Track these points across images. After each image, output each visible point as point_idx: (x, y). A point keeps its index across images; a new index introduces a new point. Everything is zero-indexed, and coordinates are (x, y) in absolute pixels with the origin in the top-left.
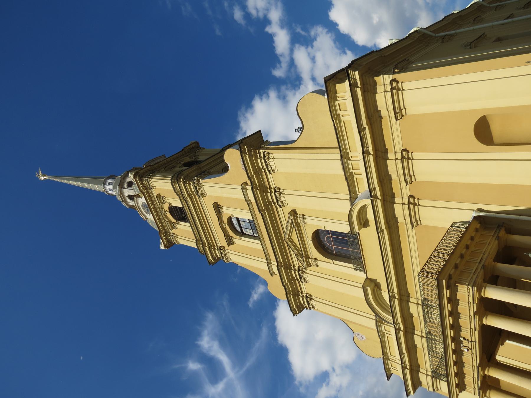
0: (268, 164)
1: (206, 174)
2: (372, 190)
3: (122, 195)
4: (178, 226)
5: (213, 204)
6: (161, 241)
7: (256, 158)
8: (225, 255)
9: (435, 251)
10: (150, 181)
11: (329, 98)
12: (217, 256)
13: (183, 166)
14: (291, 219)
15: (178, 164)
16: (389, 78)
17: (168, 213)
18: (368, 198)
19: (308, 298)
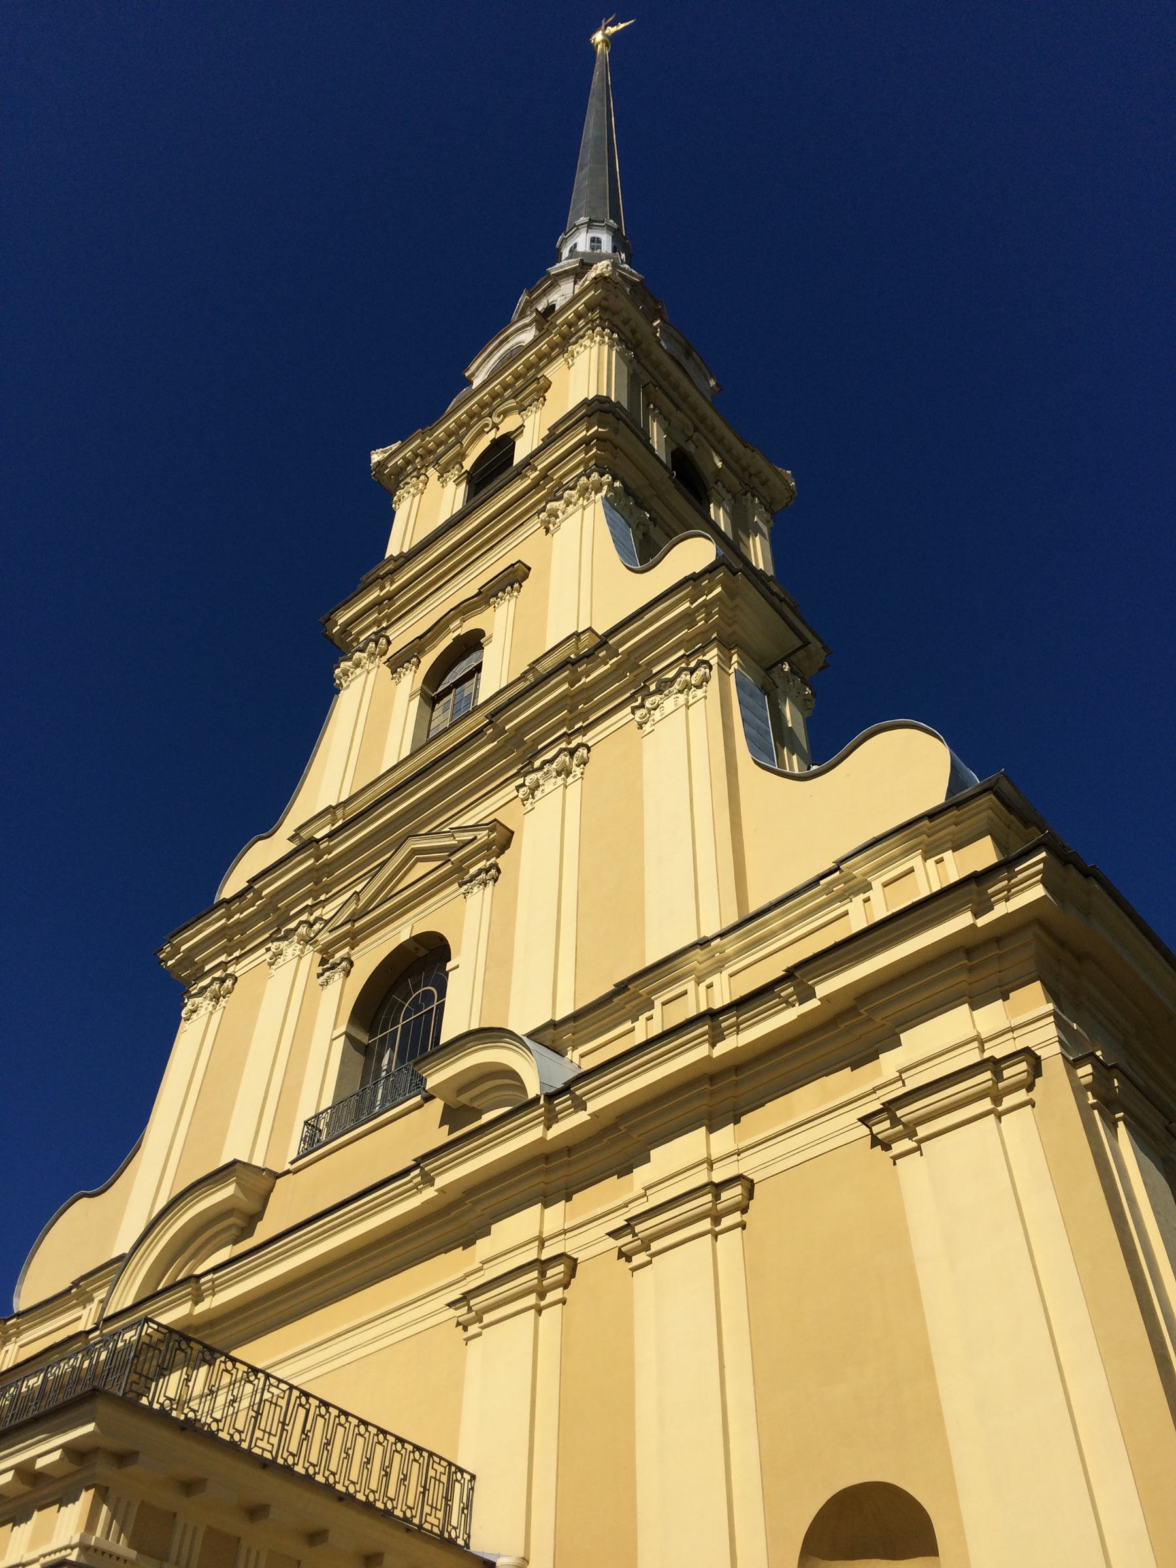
0: (666, 692)
3: (551, 285)
4: (451, 485)
5: (519, 561)
6: (394, 446)
9: (296, 1393)
10: (592, 339)
11: (926, 822)
13: (675, 447)
14: (475, 838)
15: (684, 434)
16: (1045, 1044)
17: (493, 435)
18: (542, 1084)
19: (220, 987)
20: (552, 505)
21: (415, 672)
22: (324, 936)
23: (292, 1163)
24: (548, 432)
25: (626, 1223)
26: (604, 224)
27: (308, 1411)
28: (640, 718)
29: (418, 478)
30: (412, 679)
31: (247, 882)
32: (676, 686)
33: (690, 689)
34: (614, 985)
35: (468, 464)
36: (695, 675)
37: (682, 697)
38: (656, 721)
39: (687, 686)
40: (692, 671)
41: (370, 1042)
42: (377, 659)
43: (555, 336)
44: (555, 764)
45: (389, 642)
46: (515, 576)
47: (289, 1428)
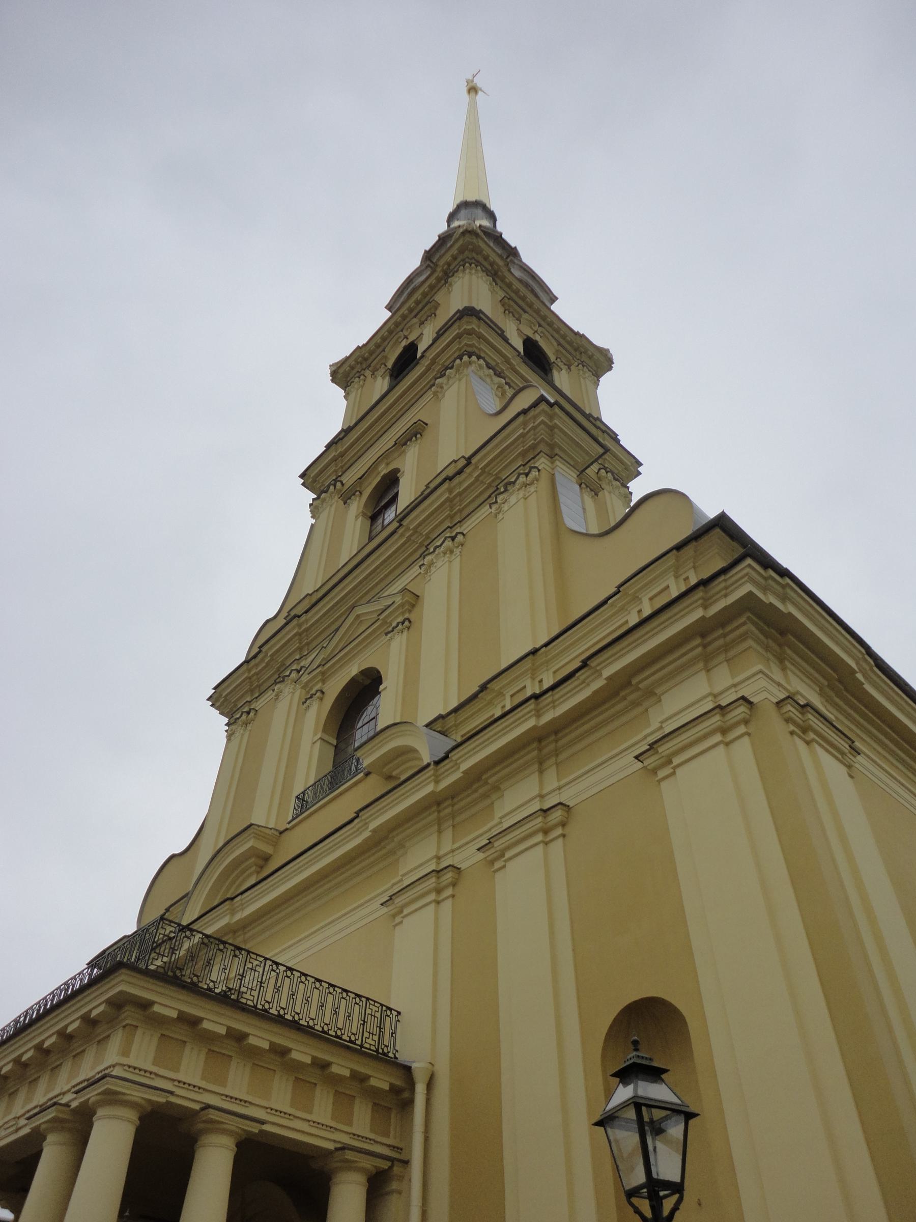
1: (492, 380)
4: (379, 379)
5: (419, 420)
8: (324, 500)
13: (525, 337)
15: (532, 329)
17: (404, 343)
18: (431, 754)
23: (289, 823)
25: (488, 841)
27: (278, 974)
30: (356, 506)
32: (517, 486)
33: (526, 487)
34: (479, 686)
35: (390, 364)
36: (528, 477)
37: (521, 493)
39: (526, 485)
40: (527, 475)
44: (442, 547)
45: (343, 484)
47: (265, 985)
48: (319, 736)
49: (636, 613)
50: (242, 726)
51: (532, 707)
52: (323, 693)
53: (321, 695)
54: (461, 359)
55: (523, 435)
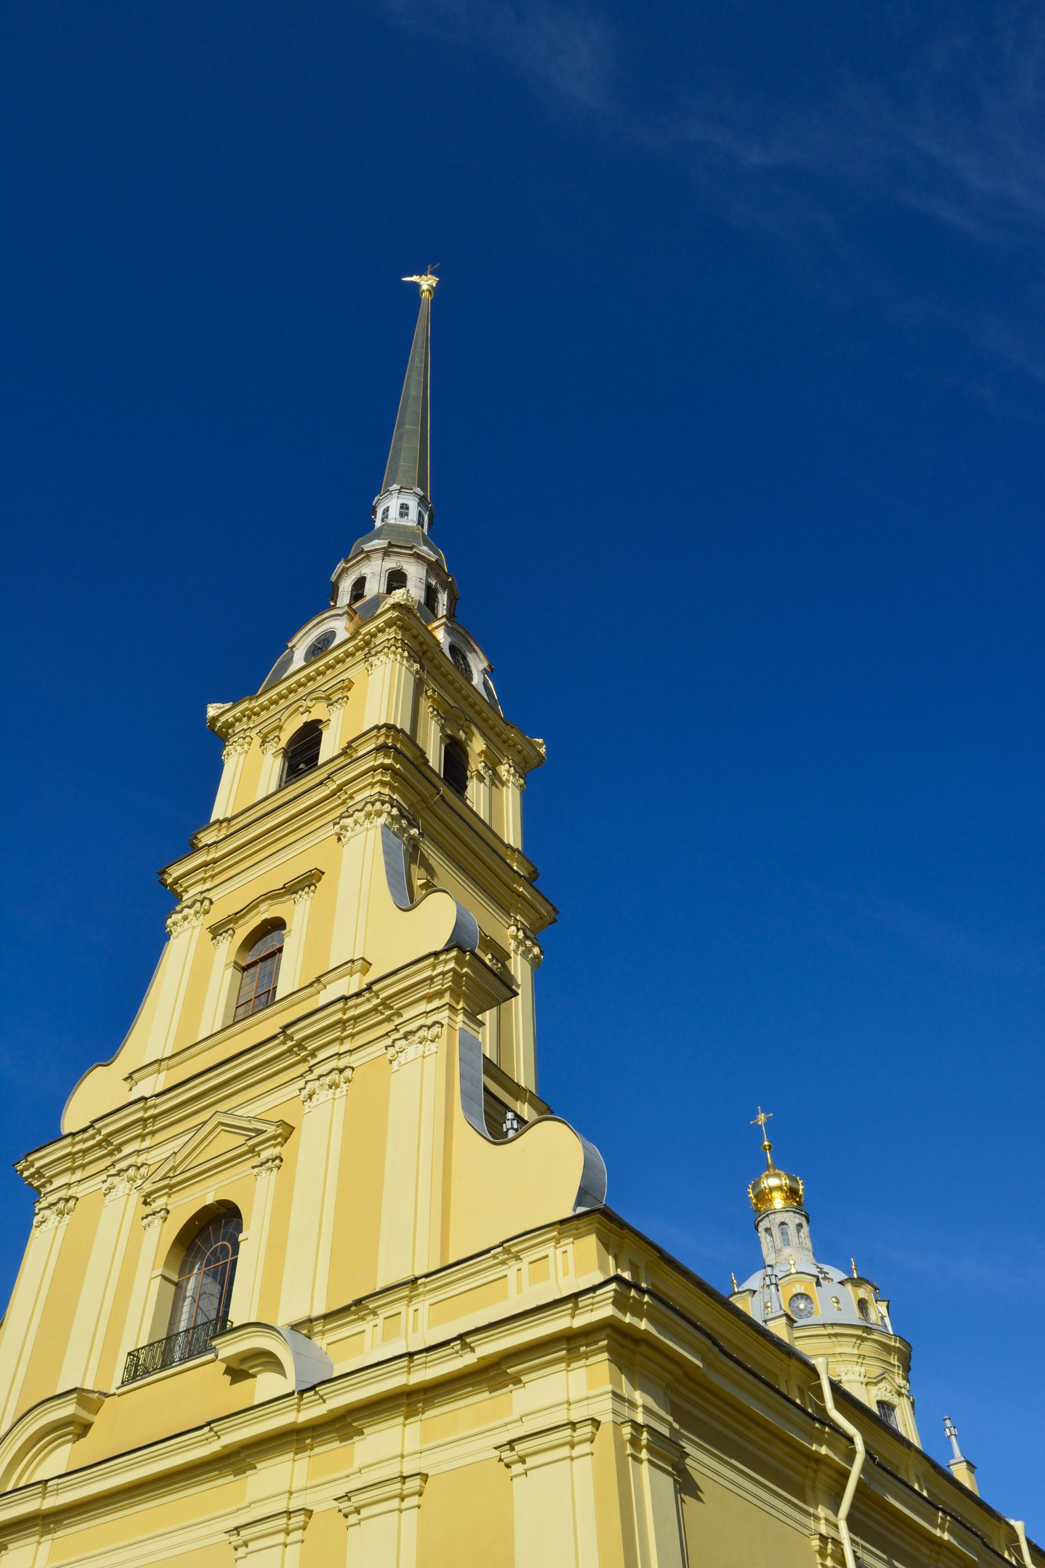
2: (316, 1393)
3: (364, 558)
4: (269, 755)
7: (430, 998)
12: (186, 891)
13: (448, 741)
14: (266, 1131)
19: (64, 1206)
20: (343, 822)
21: (231, 942)
22: (147, 1186)
23: (118, 1388)
24: (347, 745)
26: (411, 491)
28: (391, 1057)
29: (244, 739)
30: (228, 948)
31: (90, 1122)
35: (283, 743)
38: (401, 1064)
40: (429, 1027)
41: (179, 1280)
42: (201, 917)
43: (360, 642)
46: (309, 880)
48: (159, 1271)
49: (516, 1270)
50: (58, 1215)
51: (406, 1363)
52: (168, 1212)
53: (165, 1215)
54: (373, 805)
55: (431, 979)
